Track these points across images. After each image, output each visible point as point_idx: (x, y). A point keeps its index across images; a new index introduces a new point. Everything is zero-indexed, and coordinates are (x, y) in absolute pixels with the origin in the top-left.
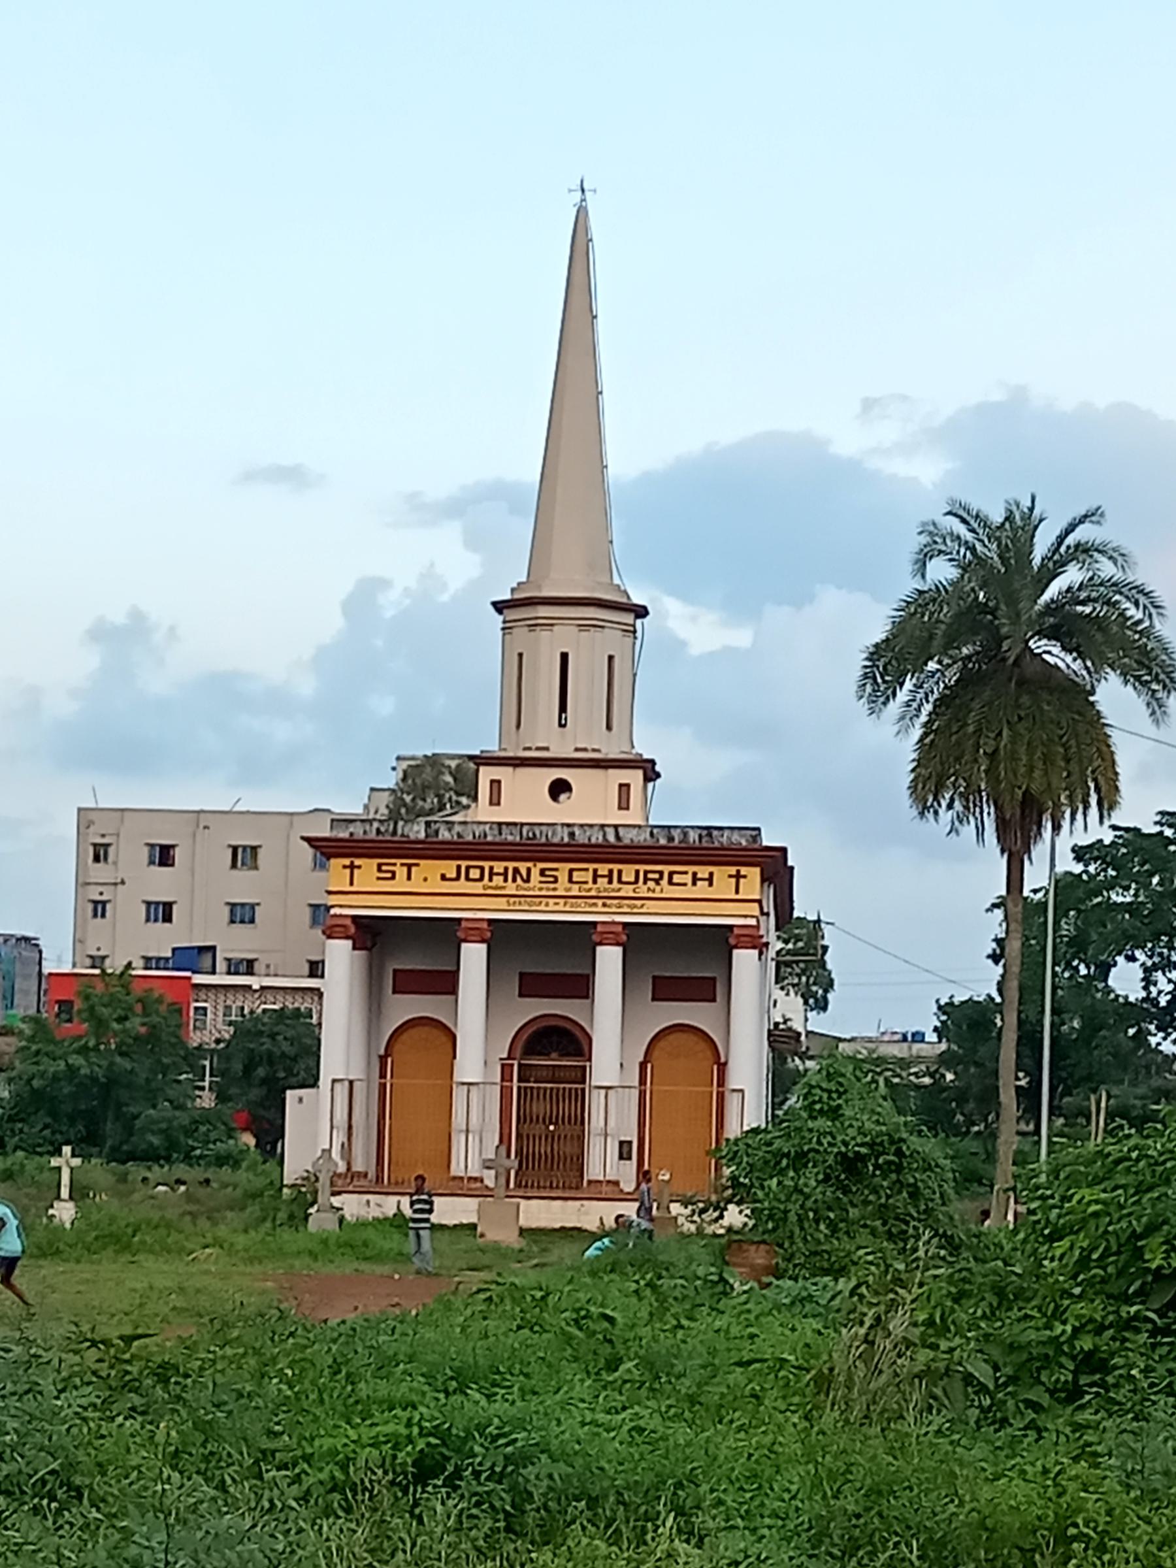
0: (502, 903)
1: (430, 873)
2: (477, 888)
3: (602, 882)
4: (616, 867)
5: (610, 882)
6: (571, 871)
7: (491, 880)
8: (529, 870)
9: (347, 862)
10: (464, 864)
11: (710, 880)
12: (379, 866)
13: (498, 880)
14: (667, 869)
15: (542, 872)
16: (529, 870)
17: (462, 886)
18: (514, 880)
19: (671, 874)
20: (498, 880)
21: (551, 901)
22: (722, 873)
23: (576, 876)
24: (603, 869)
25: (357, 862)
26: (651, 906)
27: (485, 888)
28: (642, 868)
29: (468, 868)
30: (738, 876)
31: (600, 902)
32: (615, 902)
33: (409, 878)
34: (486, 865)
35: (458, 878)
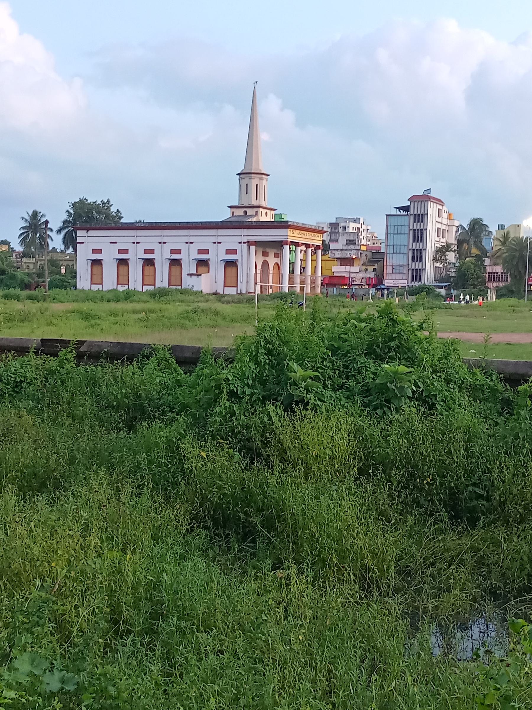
26: (315, 241)
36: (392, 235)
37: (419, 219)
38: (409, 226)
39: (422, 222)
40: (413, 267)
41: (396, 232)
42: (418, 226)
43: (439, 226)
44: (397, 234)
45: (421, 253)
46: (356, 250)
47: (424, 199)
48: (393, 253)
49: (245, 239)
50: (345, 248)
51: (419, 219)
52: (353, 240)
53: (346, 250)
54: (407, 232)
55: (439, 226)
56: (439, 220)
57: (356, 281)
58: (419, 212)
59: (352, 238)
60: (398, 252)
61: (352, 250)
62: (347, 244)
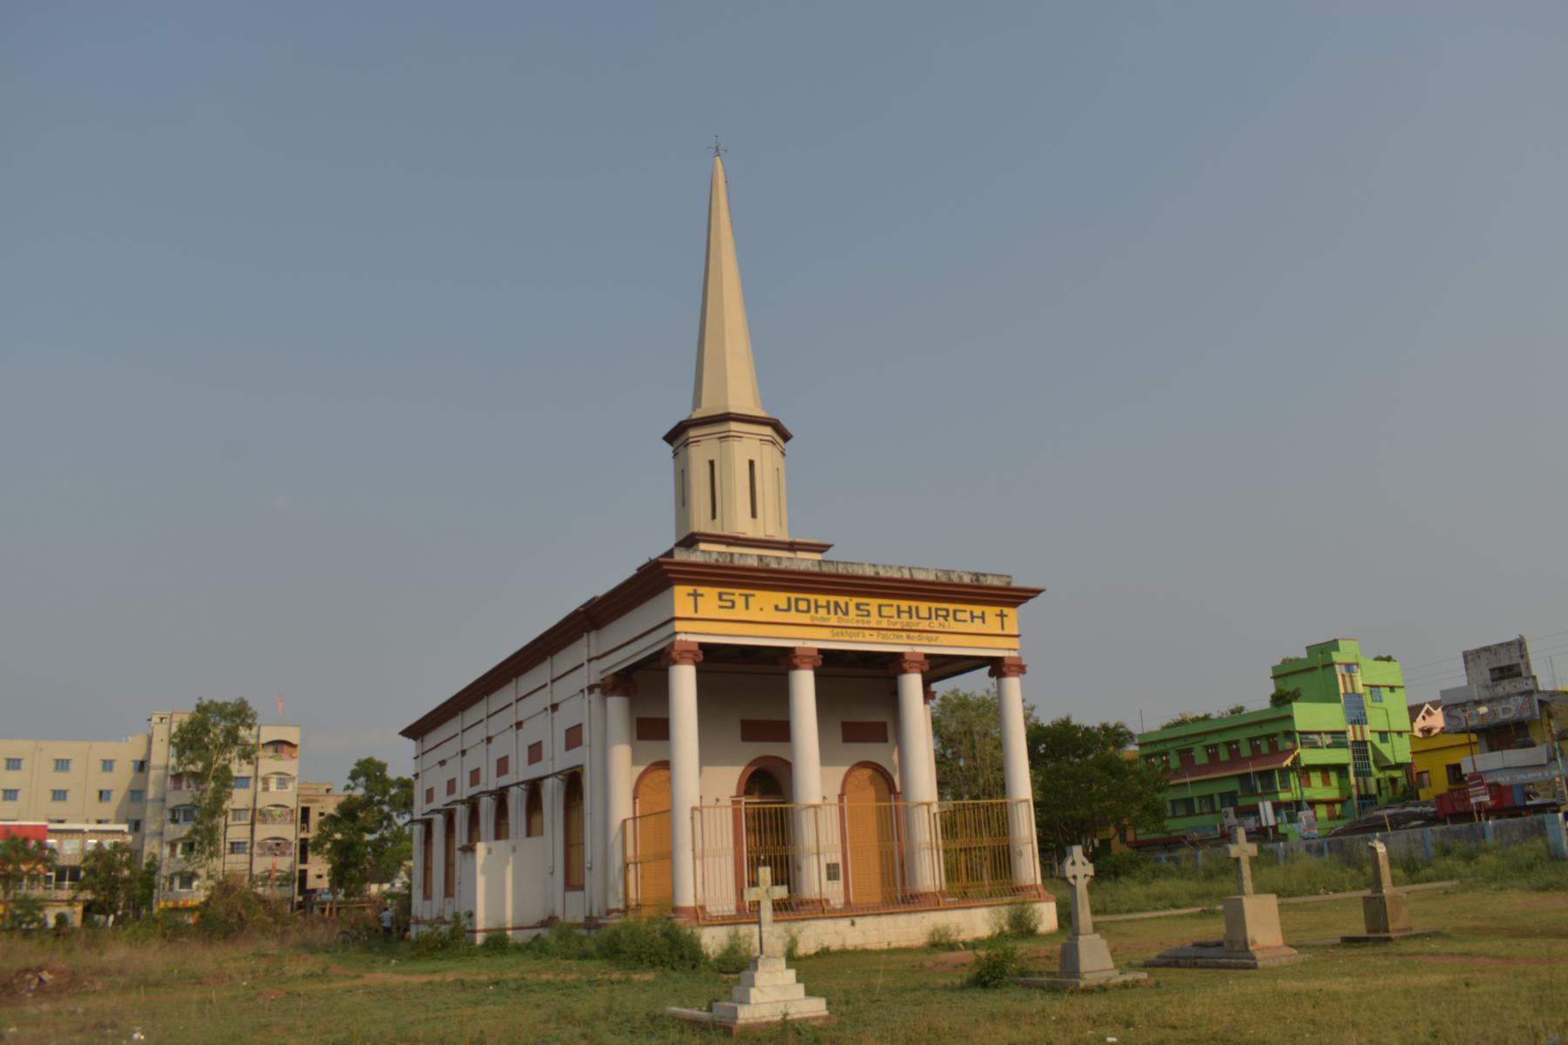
0: (826, 633)
1: (765, 603)
2: (805, 618)
3: (905, 616)
4: (914, 604)
6: (880, 606)
9: (690, 589)
10: (793, 596)
11: (983, 617)
12: (720, 595)
13: (822, 612)
14: (951, 607)
15: (858, 606)
17: (792, 617)
19: (955, 611)
20: (822, 612)
22: (991, 611)
23: (885, 611)
24: (904, 604)
25: (701, 590)
26: (943, 639)
28: (934, 605)
29: (797, 600)
30: (1002, 615)
33: (747, 607)
34: (812, 597)
35: (789, 609)
46: (1522, 694)
49: (593, 673)
50: (1486, 694)
52: (1510, 668)
57: (1536, 795)
59: (1505, 662)
61: (1508, 696)
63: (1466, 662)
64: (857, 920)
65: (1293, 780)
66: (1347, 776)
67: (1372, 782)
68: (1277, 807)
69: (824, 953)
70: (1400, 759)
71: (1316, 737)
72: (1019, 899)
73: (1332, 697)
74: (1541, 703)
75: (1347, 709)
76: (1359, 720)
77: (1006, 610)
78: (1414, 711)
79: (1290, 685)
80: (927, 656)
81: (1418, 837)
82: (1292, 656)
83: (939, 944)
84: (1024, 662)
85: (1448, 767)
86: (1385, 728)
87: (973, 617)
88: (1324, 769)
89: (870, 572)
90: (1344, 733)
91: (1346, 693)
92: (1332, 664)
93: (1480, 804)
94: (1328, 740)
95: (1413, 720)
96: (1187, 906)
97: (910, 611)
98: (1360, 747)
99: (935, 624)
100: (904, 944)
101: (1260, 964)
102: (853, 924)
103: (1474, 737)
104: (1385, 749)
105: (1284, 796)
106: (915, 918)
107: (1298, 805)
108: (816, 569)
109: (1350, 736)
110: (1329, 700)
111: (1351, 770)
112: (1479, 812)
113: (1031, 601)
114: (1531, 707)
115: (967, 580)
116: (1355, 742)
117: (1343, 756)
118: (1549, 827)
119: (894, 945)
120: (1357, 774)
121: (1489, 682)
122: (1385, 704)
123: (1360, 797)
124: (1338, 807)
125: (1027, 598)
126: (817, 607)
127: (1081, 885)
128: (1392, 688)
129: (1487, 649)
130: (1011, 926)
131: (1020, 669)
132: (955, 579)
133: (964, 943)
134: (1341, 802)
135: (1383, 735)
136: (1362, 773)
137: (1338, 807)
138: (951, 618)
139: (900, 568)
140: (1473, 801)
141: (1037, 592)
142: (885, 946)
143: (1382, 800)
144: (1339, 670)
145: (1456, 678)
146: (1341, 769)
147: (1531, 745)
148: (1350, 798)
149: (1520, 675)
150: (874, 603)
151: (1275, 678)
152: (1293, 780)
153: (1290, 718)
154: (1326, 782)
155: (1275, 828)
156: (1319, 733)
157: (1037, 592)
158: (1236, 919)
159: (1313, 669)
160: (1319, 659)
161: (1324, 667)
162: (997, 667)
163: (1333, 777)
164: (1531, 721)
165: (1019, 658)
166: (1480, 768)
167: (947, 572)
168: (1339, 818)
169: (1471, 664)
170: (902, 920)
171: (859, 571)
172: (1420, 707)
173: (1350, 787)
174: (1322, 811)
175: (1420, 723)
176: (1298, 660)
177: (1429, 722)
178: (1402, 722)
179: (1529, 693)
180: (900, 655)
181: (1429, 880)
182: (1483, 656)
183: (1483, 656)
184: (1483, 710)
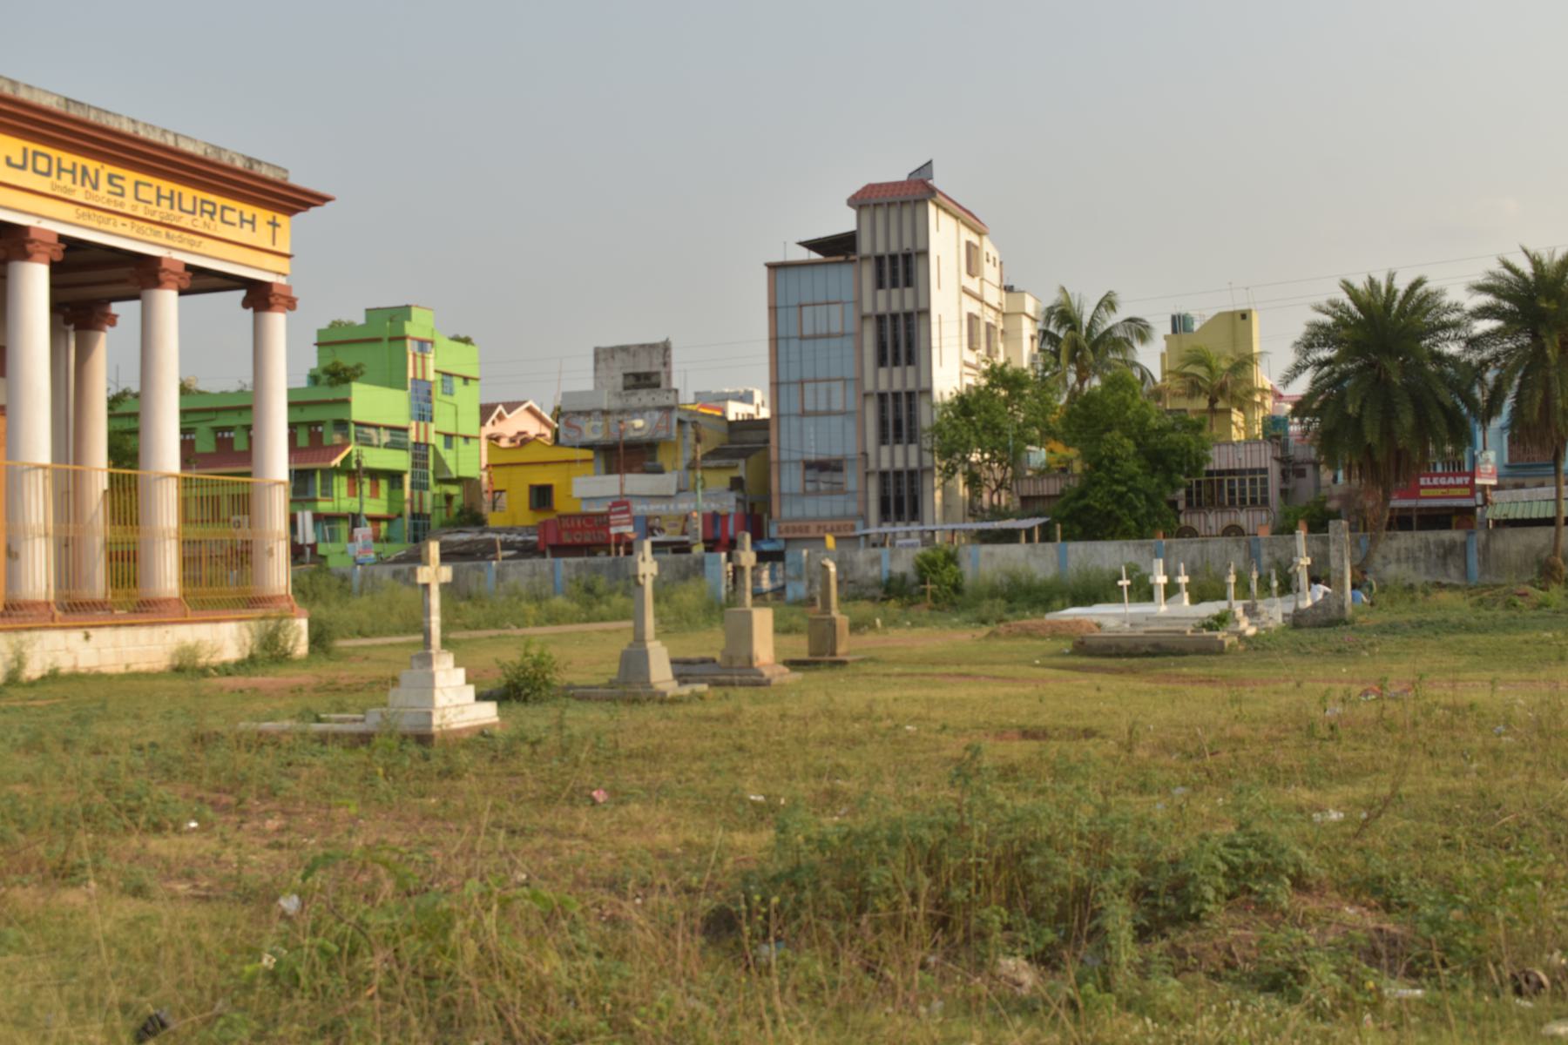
0: (68, 212)
4: (177, 188)
5: (172, 207)
6: (137, 183)
7: (59, 177)
8: (97, 172)
10: (32, 147)
11: (253, 223)
13: (67, 178)
14: (220, 201)
15: (111, 177)
16: (97, 172)
17: (27, 179)
18: (83, 184)
20: (67, 178)
21: (120, 220)
22: (263, 215)
24: (167, 187)
26: (209, 246)
27: (55, 187)
28: (201, 195)
30: (274, 224)
31: (163, 230)
32: (177, 233)
34: (55, 153)
35: (23, 167)
36: (794, 344)
37: (894, 272)
38: (858, 302)
39: (908, 283)
40: (885, 465)
41: (808, 331)
42: (894, 301)
43: (974, 307)
44: (815, 337)
45: (911, 407)
46: (659, 409)
47: (913, 195)
48: (804, 414)
50: (616, 404)
51: (894, 272)
52: (648, 376)
53: (622, 412)
54: (851, 326)
55: (974, 307)
56: (973, 284)
57: (661, 530)
58: (894, 248)
59: (643, 368)
60: (822, 407)
62: (626, 388)
63: (597, 361)
64: (92, 632)
65: (341, 485)
66: (401, 486)
67: (428, 496)
68: (318, 518)
69: (53, 677)
70: (463, 473)
71: (372, 432)
72: (274, 612)
73: (394, 379)
74: (681, 422)
75: (415, 397)
76: (424, 414)
77: (281, 219)
78: (486, 411)
79: (347, 358)
80: (188, 267)
81: (547, 569)
82: (345, 319)
83: (185, 668)
84: (294, 294)
85: (532, 487)
86: (451, 430)
87: (242, 221)
88: (375, 474)
89: (127, 128)
90: (405, 430)
91: (415, 379)
92: (403, 338)
93: (620, 536)
94: (386, 437)
95: (483, 423)
96: (397, 632)
97: (171, 199)
98: (420, 451)
99: (199, 223)
100: (143, 667)
101: (775, 681)
102: (87, 637)
103: (589, 454)
104: (448, 456)
105: (324, 506)
106: (158, 632)
107: (354, 519)
108: (61, 109)
109: (412, 436)
110: (391, 385)
111: (407, 479)
112: (617, 545)
113: (313, 210)
114: (668, 427)
115: (239, 164)
116: (417, 444)
117: (399, 460)
118: (708, 567)
119: (134, 668)
120: (413, 485)
121: (620, 389)
122: (455, 399)
123: (413, 516)
124: (384, 525)
125: (308, 205)
126: (60, 170)
127: (648, 585)
128: (466, 379)
129: (625, 349)
130: (264, 647)
131: (290, 304)
132: (225, 160)
133: (216, 669)
134: (388, 519)
135: (449, 438)
136: (419, 486)
137: (384, 525)
138: (217, 217)
139: (164, 132)
140: (613, 531)
141: (324, 199)
142: (122, 669)
143: (435, 522)
144: (411, 347)
145: (581, 379)
146: (395, 477)
147: (660, 471)
148: (400, 515)
149: (658, 386)
150: (131, 177)
151: (319, 344)
152: (341, 485)
153: (346, 402)
154: (375, 493)
155: (314, 547)
156: (377, 427)
157: (324, 199)
158: (743, 633)
159: (377, 340)
160: (386, 330)
161: (392, 339)
162: (259, 296)
163: (384, 485)
164: (666, 442)
165: (289, 288)
166: (627, 491)
167: (218, 150)
168: (388, 540)
169: (602, 365)
170: (143, 633)
171: (113, 124)
172: (492, 407)
173: (403, 502)
174: (364, 531)
175: (489, 429)
176: (350, 325)
177: (499, 428)
178: (470, 424)
179: (668, 409)
180: (155, 260)
181: (603, 619)
182: (619, 356)
183: (619, 356)
184: (639, 423)
